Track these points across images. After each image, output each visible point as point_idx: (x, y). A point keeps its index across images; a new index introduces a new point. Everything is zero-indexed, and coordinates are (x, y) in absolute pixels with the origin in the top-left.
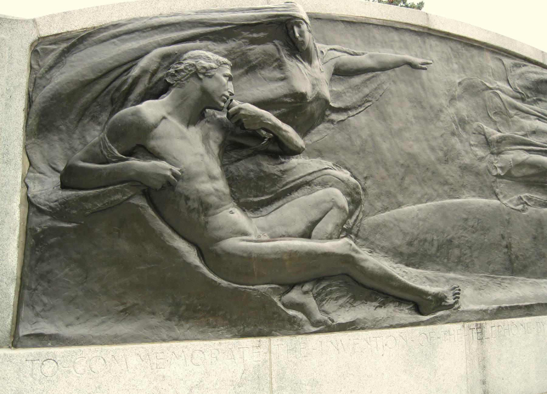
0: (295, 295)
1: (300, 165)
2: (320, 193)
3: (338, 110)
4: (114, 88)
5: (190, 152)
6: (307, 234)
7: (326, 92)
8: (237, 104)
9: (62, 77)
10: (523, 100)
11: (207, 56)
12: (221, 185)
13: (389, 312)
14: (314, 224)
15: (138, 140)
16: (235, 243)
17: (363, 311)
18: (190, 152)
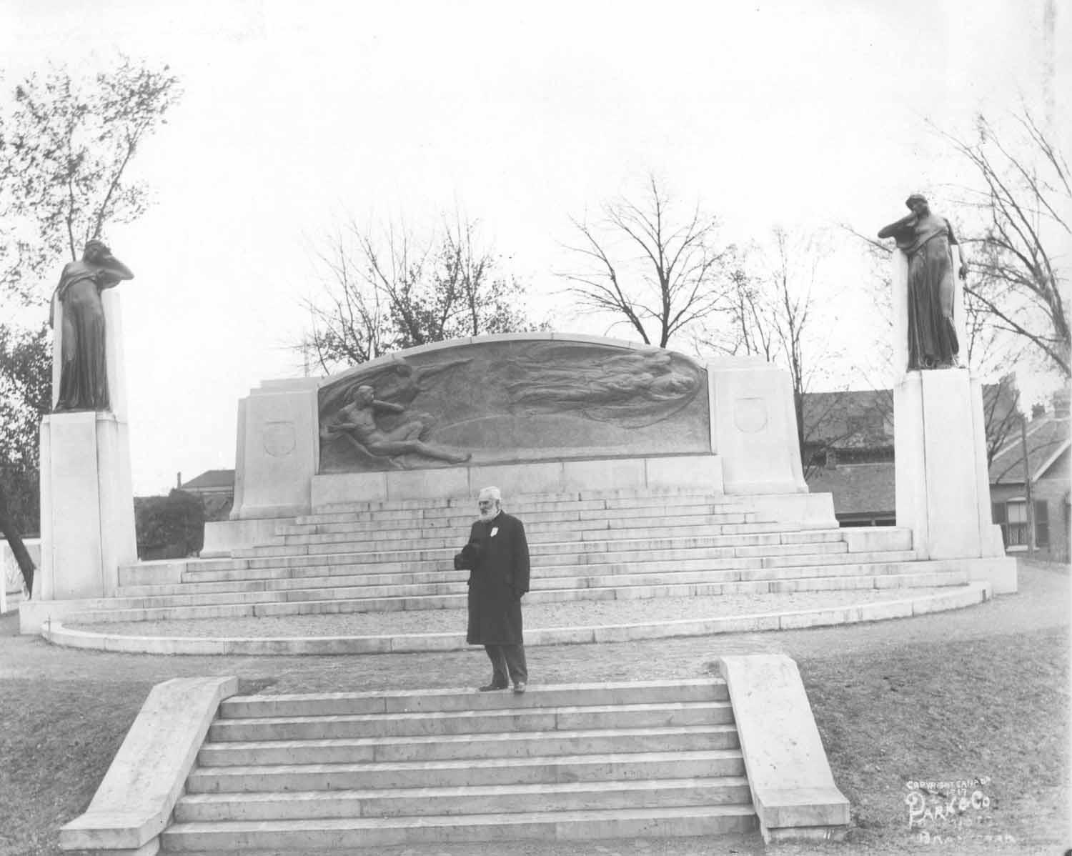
0: (398, 459)
1: (409, 414)
2: (411, 424)
3: (424, 391)
4: (342, 400)
5: (362, 418)
6: (405, 439)
7: (416, 386)
8: (375, 401)
9: (326, 401)
10: (538, 362)
11: (365, 388)
12: (373, 427)
13: (436, 464)
14: (408, 435)
15: (345, 418)
16: (377, 444)
17: (427, 463)
18: (362, 418)
